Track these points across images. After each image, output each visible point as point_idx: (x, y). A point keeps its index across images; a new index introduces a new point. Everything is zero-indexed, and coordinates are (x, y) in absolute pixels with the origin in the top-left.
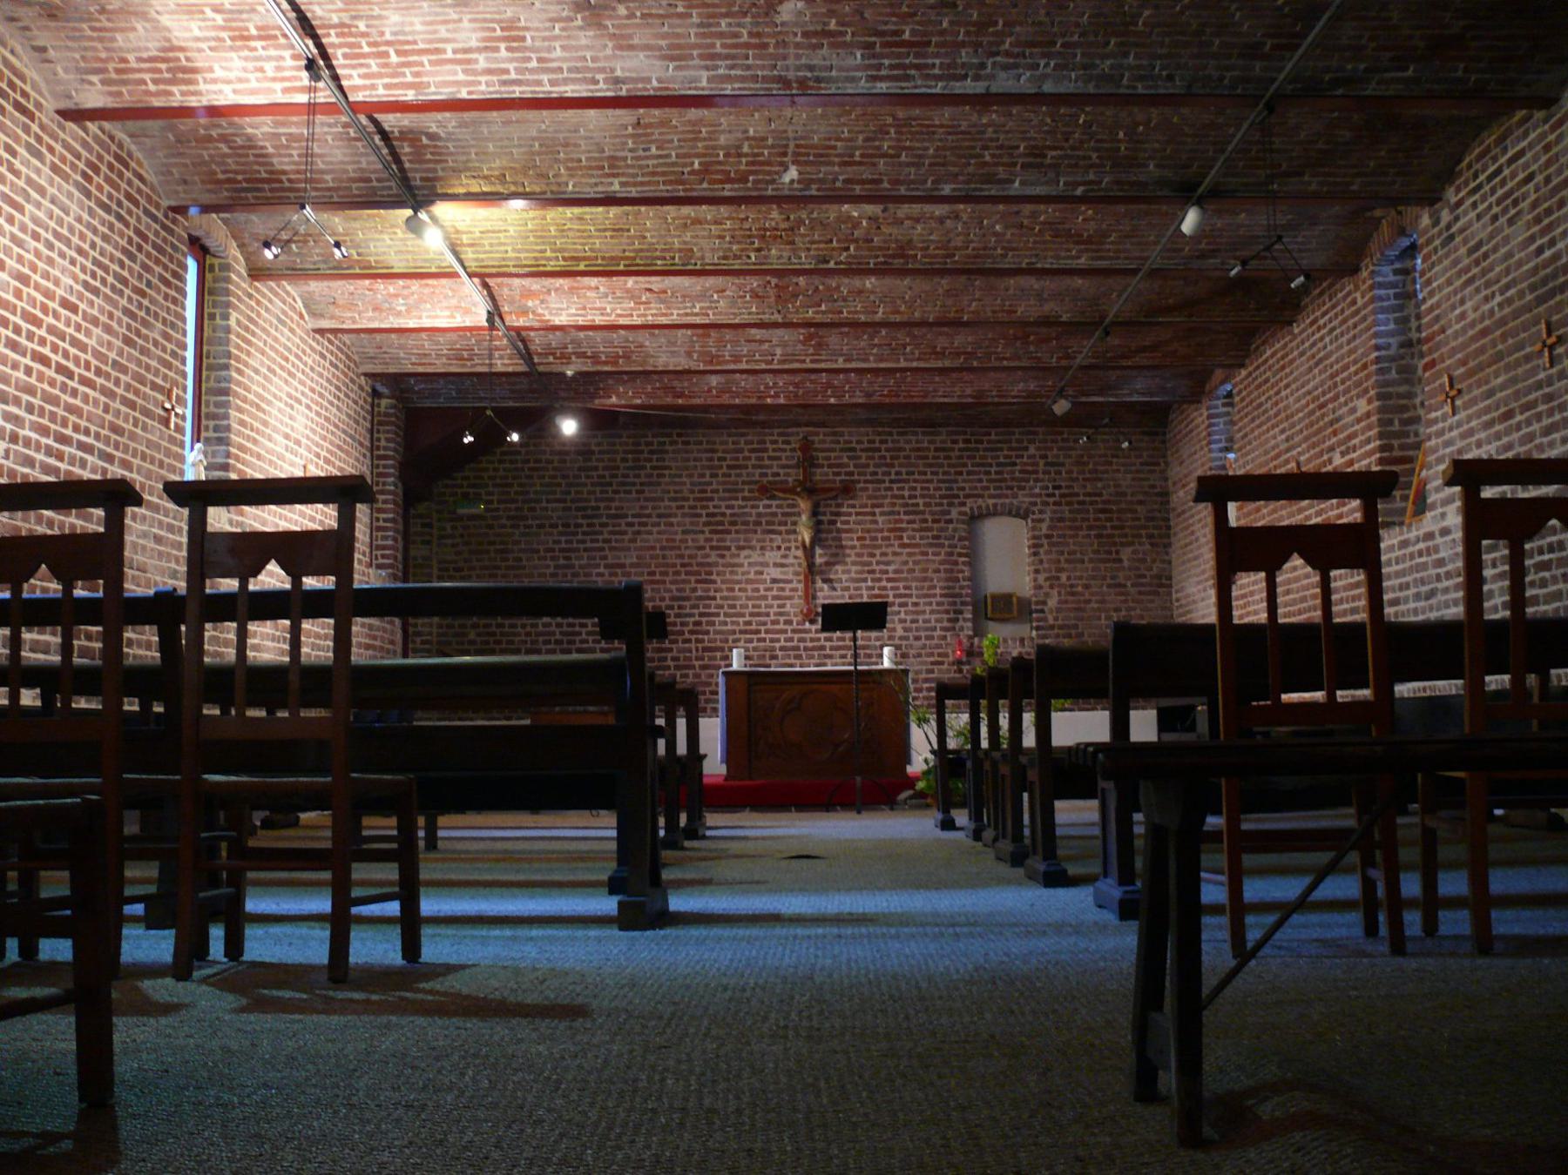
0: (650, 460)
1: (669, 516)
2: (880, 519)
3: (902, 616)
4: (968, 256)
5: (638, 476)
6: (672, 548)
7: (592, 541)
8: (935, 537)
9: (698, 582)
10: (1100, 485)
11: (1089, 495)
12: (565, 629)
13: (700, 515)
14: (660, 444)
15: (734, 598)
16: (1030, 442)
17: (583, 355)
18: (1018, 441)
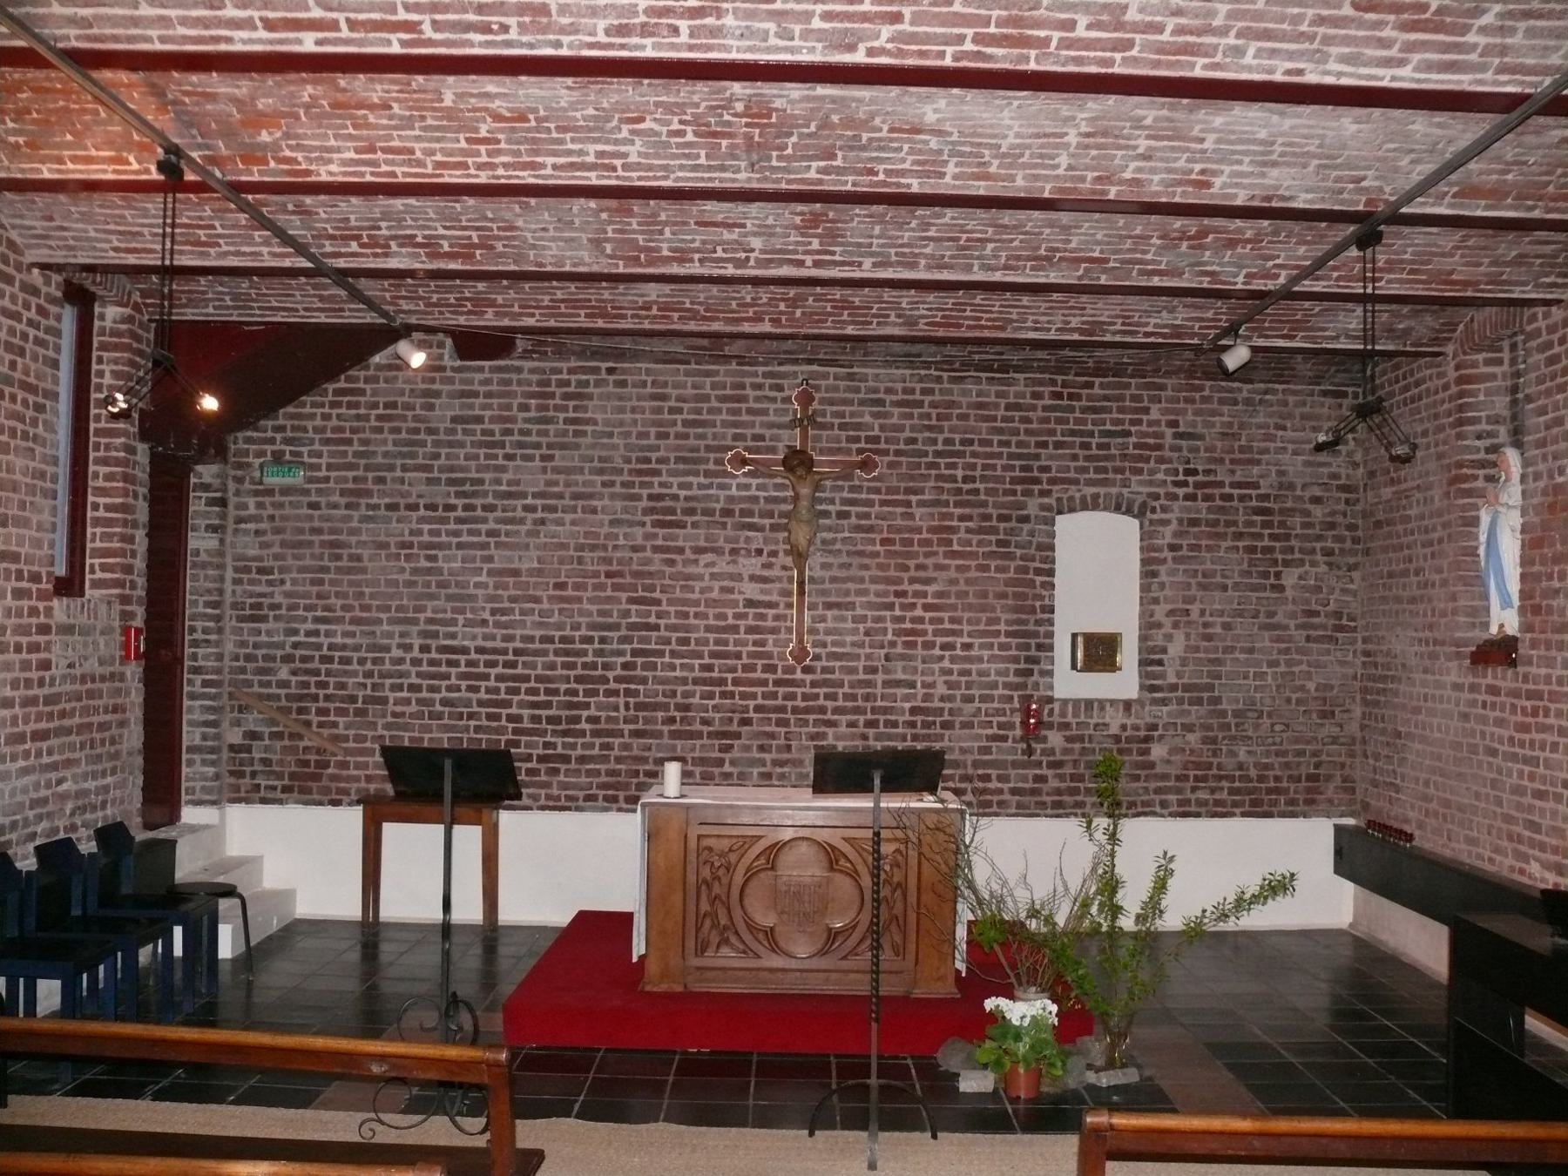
0: (565, 409)
1: (591, 496)
2: (918, 512)
3: (946, 664)
4: (1162, 49)
5: (545, 433)
6: (593, 548)
7: (471, 532)
8: (1000, 543)
9: (631, 601)
10: (1256, 470)
11: (1239, 485)
12: (425, 668)
13: (638, 498)
14: (580, 384)
15: (688, 629)
16: (1153, 399)
17: (408, 241)
18: (1135, 398)
